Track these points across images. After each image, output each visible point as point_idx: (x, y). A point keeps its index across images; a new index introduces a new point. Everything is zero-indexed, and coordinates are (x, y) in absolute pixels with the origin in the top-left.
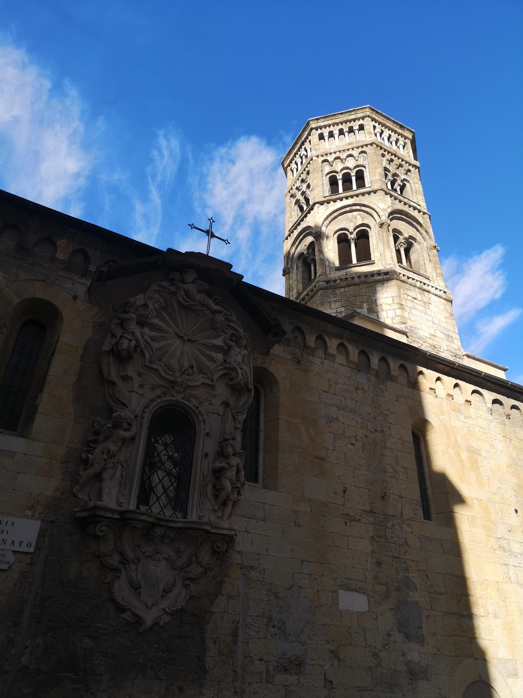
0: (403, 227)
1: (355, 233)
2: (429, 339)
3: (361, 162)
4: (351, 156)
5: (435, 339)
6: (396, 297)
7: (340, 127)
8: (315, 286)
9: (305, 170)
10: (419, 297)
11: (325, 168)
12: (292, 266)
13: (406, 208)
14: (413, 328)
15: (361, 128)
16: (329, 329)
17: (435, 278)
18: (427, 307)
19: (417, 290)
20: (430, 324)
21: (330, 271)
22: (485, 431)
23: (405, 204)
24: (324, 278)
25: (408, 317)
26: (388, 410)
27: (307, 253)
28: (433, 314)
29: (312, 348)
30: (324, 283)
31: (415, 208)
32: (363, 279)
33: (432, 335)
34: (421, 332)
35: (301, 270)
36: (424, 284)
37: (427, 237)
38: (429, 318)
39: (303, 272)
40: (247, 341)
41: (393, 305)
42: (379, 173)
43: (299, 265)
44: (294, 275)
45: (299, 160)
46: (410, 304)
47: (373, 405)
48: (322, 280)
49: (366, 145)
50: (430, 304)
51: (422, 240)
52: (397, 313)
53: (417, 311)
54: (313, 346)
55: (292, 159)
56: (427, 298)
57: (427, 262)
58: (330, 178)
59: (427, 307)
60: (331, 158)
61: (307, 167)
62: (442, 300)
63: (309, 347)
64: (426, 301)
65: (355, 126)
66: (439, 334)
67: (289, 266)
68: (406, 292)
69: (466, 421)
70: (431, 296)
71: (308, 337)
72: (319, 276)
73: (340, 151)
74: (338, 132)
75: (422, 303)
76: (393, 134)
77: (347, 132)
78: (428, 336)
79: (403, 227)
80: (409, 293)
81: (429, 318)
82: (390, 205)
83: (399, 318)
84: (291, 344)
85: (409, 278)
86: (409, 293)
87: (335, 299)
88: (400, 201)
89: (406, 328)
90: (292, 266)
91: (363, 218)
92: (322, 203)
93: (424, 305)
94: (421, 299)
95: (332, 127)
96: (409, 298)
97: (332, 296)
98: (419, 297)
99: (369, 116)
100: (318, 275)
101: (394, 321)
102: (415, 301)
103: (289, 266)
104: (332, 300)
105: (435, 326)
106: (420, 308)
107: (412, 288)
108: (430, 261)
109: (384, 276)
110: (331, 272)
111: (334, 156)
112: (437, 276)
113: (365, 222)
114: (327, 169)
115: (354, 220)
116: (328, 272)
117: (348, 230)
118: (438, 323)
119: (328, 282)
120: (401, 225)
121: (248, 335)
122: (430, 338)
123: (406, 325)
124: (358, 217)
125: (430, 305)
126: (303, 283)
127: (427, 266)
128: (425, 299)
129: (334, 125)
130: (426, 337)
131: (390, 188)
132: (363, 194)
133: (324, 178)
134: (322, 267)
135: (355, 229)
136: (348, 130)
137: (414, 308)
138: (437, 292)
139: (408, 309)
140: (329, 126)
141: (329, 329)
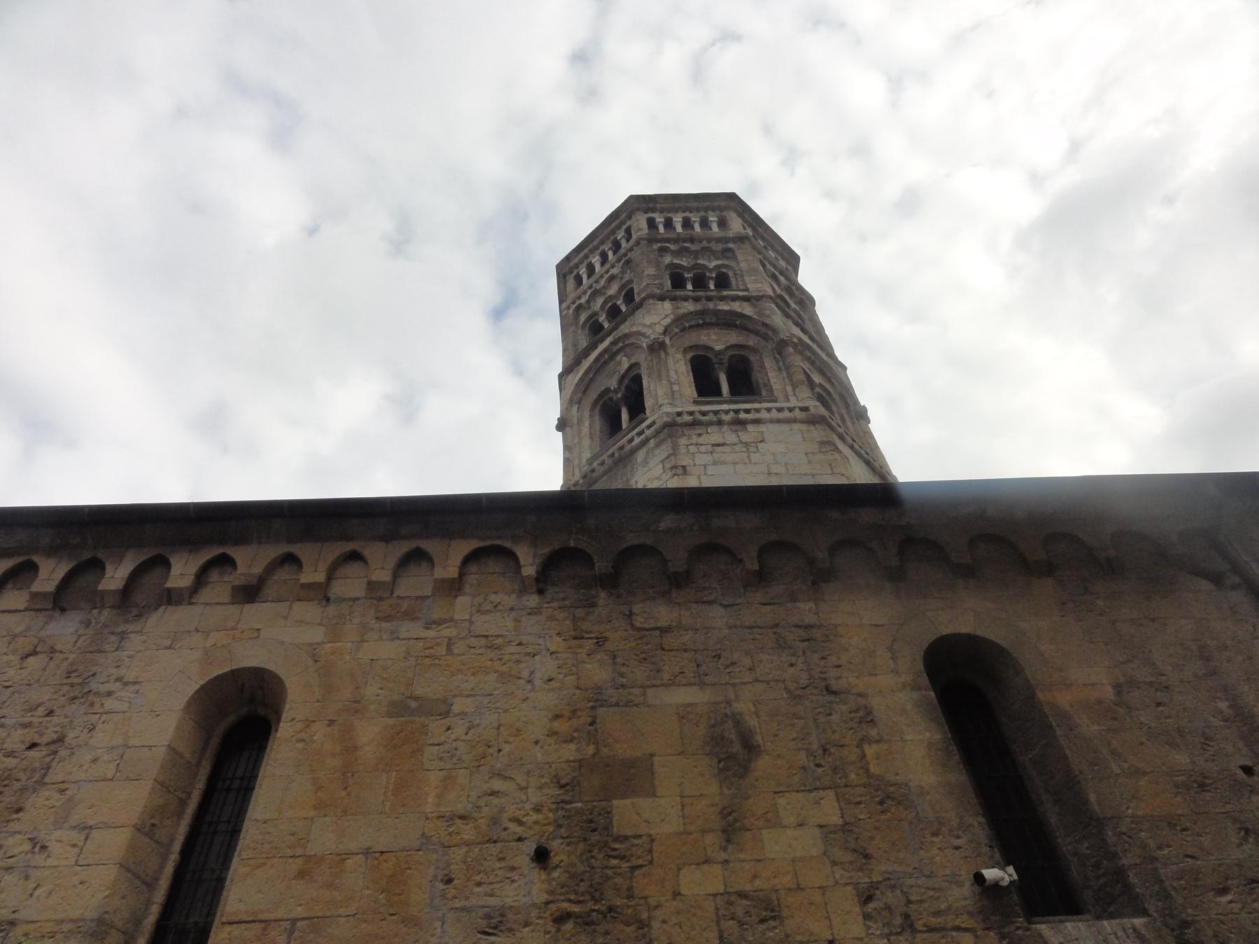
1: (623, 388)
3: (627, 277)
13: (711, 305)
22: (500, 641)
26: (118, 680)
31: (734, 299)
47: (69, 681)
51: (763, 342)
62: (796, 426)
69: (431, 633)
70: (763, 428)
76: (690, 215)
79: (713, 337)
80: (701, 440)
86: (701, 440)
91: (629, 357)
94: (736, 440)
96: (703, 449)
99: (638, 209)
112: (794, 390)
113: (633, 361)
114: (583, 317)
135: (621, 382)
137: (715, 463)
138: (786, 414)
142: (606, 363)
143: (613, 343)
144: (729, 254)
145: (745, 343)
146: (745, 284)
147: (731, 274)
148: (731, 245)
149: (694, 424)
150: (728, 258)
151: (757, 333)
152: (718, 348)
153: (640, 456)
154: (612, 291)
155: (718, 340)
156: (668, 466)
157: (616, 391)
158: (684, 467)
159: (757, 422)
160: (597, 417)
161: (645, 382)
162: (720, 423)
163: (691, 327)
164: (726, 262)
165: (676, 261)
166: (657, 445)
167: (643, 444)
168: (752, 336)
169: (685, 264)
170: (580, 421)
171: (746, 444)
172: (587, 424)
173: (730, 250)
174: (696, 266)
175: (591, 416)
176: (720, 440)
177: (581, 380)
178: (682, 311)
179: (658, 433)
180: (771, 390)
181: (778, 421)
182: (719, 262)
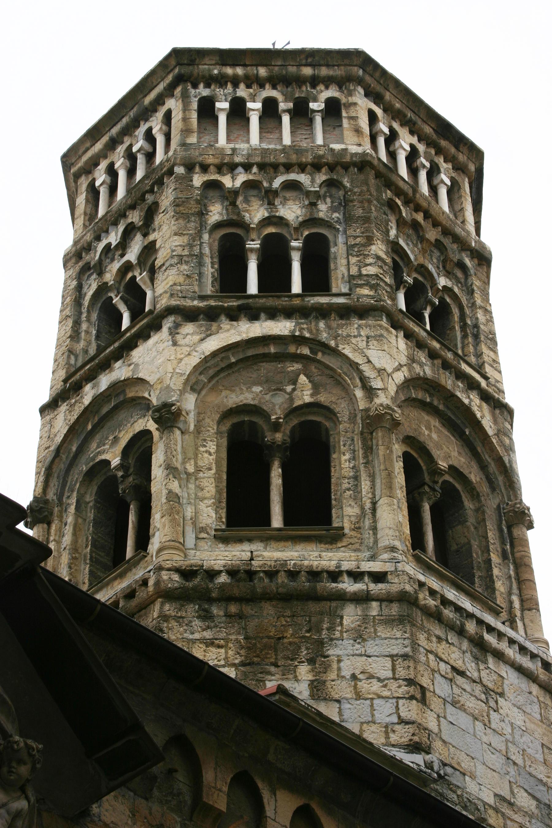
0: (434, 436)
1: (287, 429)
2: (491, 812)
4: (292, 186)
5: (508, 812)
6: (405, 657)
7: (269, 92)
8: (145, 582)
9: (143, 198)
10: (470, 667)
11: (212, 208)
12: (60, 499)
13: (448, 381)
14: (449, 770)
15: (333, 110)
16: (271, 757)
17: (518, 613)
18: (492, 704)
19: (465, 645)
20: (496, 761)
21: (197, 538)
23: (446, 365)
24: (175, 559)
25: (435, 729)
27: (121, 466)
28: (508, 730)
29: (220, 813)
30: (176, 577)
31: (472, 385)
32: (303, 583)
33: (502, 799)
34: (471, 786)
35: (91, 515)
36: (490, 629)
37: (501, 479)
38: (497, 742)
39: (96, 523)
40: (33, 769)
41: (393, 685)
42: (378, 258)
43: (88, 498)
44: (68, 530)
45: (120, 164)
46: (442, 688)
48: (168, 565)
49: (346, 167)
50: (502, 695)
52: (404, 714)
53: (462, 714)
54: (222, 805)
55: (103, 154)
56: (495, 677)
57: (495, 558)
58: (224, 237)
59: (492, 704)
60: (233, 179)
61: (151, 191)
62: (535, 689)
63: (209, 809)
64: (490, 685)
65: (315, 100)
66: (523, 800)
67: (51, 495)
68: (434, 645)
71: (209, 775)
72: (160, 550)
73: (262, 167)
74: (258, 105)
75: (478, 689)
77: (288, 111)
78: (491, 800)
79: (434, 436)
80: (442, 649)
81: (497, 742)
82: (404, 360)
83: (411, 729)
84: (156, 793)
85: (445, 602)
87: (208, 634)
88: (433, 355)
89: (429, 765)
90: (60, 499)
91: (316, 388)
92: (190, 315)
93: (483, 697)
94: (475, 675)
95: (242, 86)
96: (442, 665)
97: (197, 623)
98: (470, 667)
100: (154, 545)
101: (394, 738)
102: (460, 680)
103: (51, 495)
104: (197, 636)
105: (512, 770)
106: (471, 704)
107: (452, 637)
108: (504, 556)
109: (372, 586)
110: (201, 543)
111: (242, 178)
113: (323, 398)
114: (216, 213)
115: (289, 388)
116: (190, 541)
117: (266, 416)
118: (520, 761)
119: (187, 574)
120: (429, 428)
121: (40, 746)
122: (496, 810)
123: (428, 757)
124: (303, 378)
125: (501, 700)
126: (94, 561)
127: (496, 572)
128: (488, 680)
129: (251, 81)
130: (485, 804)
131: (403, 307)
132: (323, 312)
133: (206, 237)
134: (174, 523)
136: (291, 105)
137: (454, 703)
138: (525, 662)
139: (435, 703)
140: (235, 82)
141: (271, 757)
142: (266, 357)
143: (294, 339)
144: (460, 274)
145: (466, 472)
146: (479, 355)
147: (456, 311)
148: (468, 262)
149: (436, 616)
150: (458, 281)
151: (483, 467)
152: (443, 464)
153: (350, 615)
154: (292, 211)
155: (447, 452)
156: (401, 672)
157: (276, 426)
158: (422, 687)
159: (499, 655)
160: (224, 442)
161: (343, 463)
162: (461, 632)
163: (414, 400)
164: (456, 290)
165: (402, 242)
166: (389, 622)
167: (362, 599)
168: (475, 466)
169: (412, 257)
170: (198, 430)
171: (487, 690)
172: (212, 447)
173: (461, 266)
174: (422, 269)
175: (219, 433)
176: (459, 664)
177: (215, 354)
178: (417, 369)
179: (386, 599)
180: (490, 587)
181: (520, 669)
182: (449, 284)
